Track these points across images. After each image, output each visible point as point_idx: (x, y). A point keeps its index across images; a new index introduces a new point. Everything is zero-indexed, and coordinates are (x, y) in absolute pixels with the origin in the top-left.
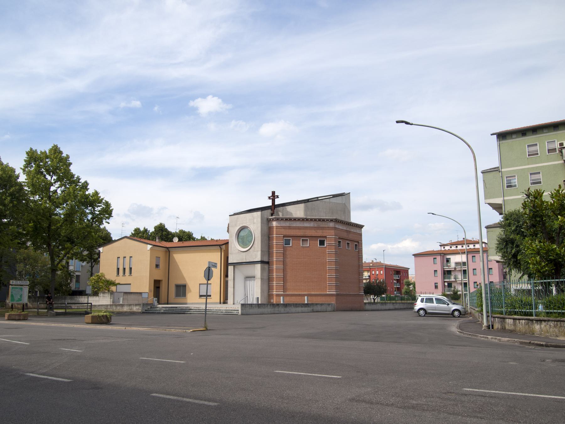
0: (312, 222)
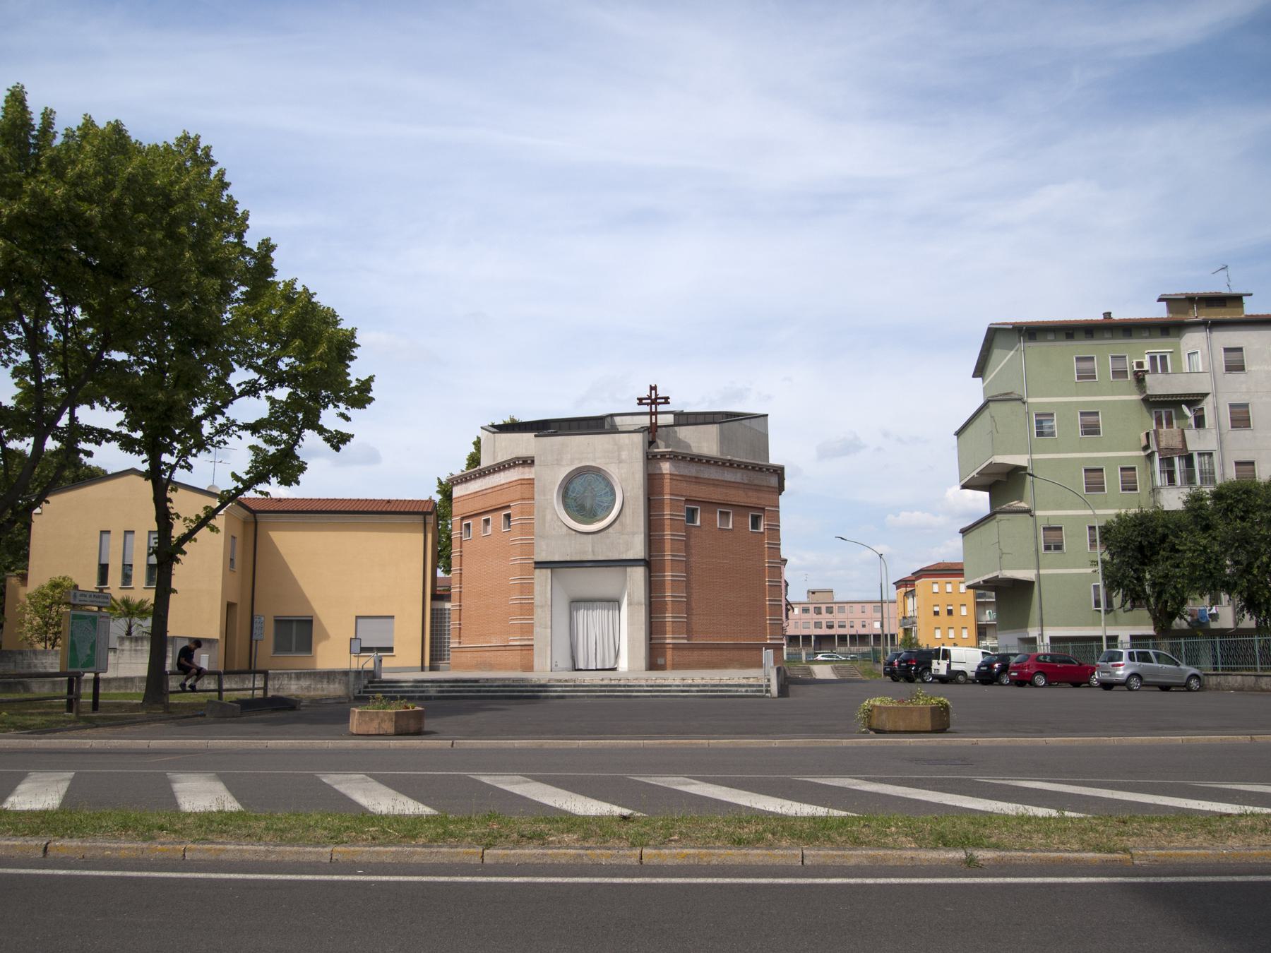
0: (738, 470)
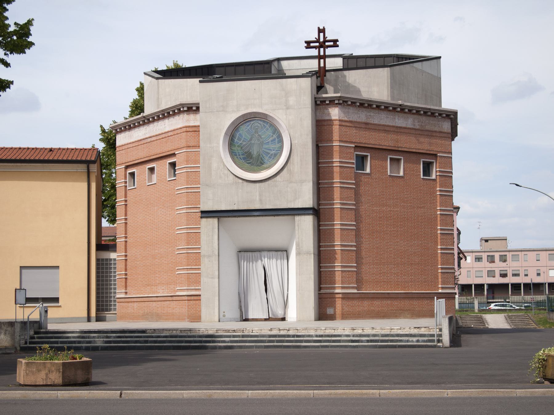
0: (409, 115)
